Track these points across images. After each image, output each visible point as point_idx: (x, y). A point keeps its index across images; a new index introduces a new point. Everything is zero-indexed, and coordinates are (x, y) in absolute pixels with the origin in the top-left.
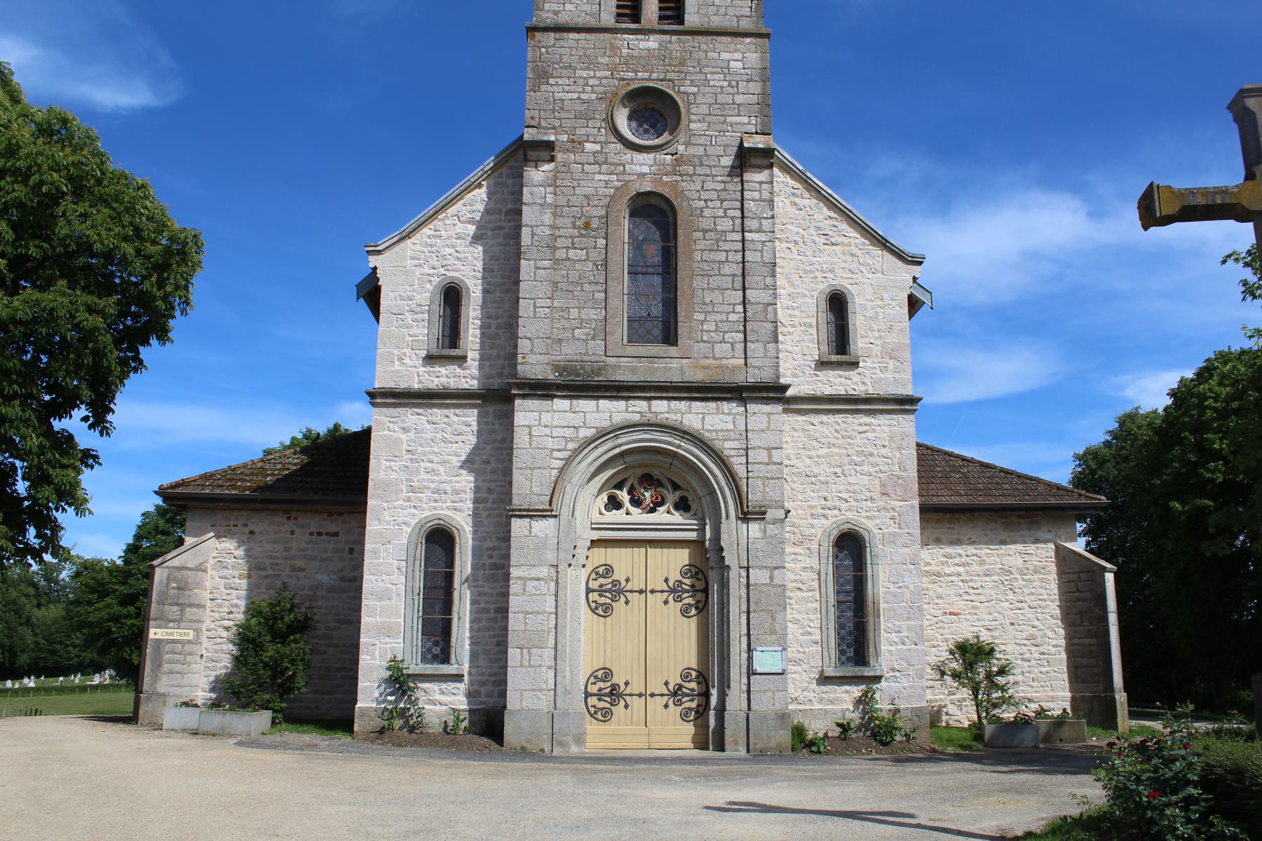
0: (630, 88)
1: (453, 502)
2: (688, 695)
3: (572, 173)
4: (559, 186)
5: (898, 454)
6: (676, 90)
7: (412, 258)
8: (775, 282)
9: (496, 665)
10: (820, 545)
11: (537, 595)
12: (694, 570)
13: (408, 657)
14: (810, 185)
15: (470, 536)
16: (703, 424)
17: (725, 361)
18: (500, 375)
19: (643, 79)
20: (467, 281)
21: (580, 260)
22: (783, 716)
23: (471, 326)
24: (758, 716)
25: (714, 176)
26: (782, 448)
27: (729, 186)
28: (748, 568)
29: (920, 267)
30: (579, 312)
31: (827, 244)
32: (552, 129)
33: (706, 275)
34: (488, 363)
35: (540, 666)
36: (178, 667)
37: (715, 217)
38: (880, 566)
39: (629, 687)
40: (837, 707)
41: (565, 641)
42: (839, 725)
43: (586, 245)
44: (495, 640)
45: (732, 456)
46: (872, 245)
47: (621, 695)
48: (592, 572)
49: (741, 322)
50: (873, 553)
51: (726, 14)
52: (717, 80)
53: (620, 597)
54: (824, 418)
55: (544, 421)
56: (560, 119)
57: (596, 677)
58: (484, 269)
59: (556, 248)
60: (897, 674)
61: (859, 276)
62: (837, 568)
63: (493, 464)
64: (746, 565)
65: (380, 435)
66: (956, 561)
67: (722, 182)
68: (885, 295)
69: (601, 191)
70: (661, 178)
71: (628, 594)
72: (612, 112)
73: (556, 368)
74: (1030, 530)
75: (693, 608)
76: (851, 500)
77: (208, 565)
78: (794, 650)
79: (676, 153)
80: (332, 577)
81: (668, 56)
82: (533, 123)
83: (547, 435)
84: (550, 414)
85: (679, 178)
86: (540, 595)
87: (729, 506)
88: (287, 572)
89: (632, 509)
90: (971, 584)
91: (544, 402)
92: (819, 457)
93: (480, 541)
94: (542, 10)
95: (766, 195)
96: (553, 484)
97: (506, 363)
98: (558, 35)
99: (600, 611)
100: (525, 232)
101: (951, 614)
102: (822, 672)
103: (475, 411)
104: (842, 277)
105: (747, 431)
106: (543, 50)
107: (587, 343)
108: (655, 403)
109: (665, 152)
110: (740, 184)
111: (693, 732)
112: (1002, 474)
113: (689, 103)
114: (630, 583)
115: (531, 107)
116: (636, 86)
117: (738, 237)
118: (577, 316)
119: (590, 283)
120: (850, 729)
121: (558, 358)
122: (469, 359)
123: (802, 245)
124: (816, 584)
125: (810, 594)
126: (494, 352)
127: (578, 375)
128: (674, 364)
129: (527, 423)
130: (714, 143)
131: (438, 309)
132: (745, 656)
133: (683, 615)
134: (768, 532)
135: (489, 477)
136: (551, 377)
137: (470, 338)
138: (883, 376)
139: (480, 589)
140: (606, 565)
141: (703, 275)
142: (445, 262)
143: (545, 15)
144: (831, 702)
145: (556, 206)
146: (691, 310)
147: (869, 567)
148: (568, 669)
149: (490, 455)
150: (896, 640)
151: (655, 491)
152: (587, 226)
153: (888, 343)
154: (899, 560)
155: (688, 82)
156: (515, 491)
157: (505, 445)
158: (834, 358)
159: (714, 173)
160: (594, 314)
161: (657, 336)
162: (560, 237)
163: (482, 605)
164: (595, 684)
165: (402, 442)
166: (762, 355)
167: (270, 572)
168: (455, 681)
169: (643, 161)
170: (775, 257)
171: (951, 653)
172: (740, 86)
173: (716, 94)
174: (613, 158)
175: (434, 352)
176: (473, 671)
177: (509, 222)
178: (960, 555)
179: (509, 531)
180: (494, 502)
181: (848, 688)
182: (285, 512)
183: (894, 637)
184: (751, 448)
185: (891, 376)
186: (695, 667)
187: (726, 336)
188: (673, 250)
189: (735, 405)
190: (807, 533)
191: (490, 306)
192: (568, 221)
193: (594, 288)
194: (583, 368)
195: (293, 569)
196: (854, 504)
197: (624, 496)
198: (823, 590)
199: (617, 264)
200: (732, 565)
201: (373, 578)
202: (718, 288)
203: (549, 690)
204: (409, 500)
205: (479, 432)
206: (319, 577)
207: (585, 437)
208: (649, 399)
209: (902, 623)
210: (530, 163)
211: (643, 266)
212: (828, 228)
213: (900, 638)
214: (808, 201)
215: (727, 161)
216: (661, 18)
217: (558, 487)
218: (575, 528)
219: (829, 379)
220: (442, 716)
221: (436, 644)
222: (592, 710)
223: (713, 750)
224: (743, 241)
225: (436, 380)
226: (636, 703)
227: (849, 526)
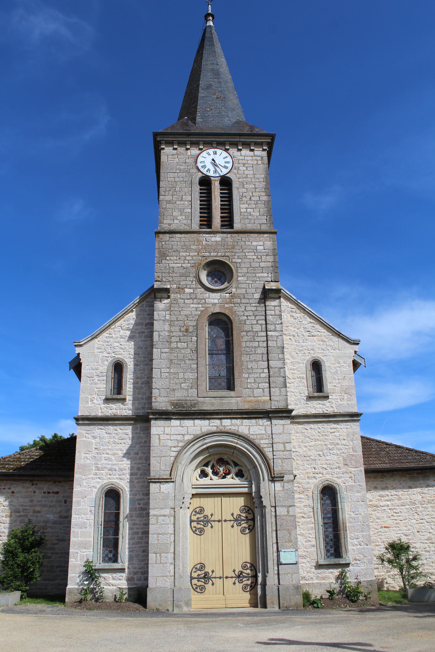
0: (207, 261)
1: (119, 475)
2: (246, 577)
3: (179, 304)
4: (173, 311)
5: (351, 443)
6: (231, 261)
7: (98, 348)
8: (284, 357)
9: (143, 563)
10: (313, 493)
11: (164, 524)
12: (247, 508)
13: (95, 560)
14: (300, 306)
15: (128, 493)
16: (249, 431)
17: (259, 398)
18: (144, 408)
19: (214, 256)
20: (126, 360)
21: (184, 348)
22: (298, 587)
23: (128, 383)
24: (284, 587)
25: (251, 304)
26: (291, 443)
28: (275, 507)
29: (358, 346)
30: (184, 375)
31: (310, 336)
32: (168, 282)
33: (248, 354)
34: (137, 402)
35: (166, 563)
38: (345, 503)
39: (214, 573)
40: (327, 581)
41: (179, 549)
42: (328, 591)
43: (187, 340)
44: (142, 549)
45: (265, 448)
46: (332, 335)
47: (209, 578)
48: (193, 511)
49: (267, 378)
50: (341, 497)
51: (254, 223)
52: (251, 256)
53: (208, 524)
54: (312, 426)
55: (166, 432)
56: (172, 277)
57: (196, 568)
58: (135, 354)
59: (172, 342)
60: (358, 562)
61: (327, 352)
62: (323, 505)
63: (140, 455)
64: (274, 505)
65: (81, 440)
66: (386, 498)
67: (255, 306)
68: (341, 361)
69: (194, 313)
70: (224, 305)
71: (212, 523)
72: (198, 273)
73: (172, 404)
74: (424, 480)
75: (247, 529)
76: (328, 468)
78: (302, 550)
79: (231, 293)
80: (55, 516)
81: (226, 244)
82: (159, 279)
83: (168, 439)
84: (170, 428)
85: (233, 305)
86: (166, 524)
87: (264, 474)
88: (31, 514)
89: (214, 477)
90: (394, 511)
91: (166, 422)
92: (310, 446)
93: (134, 495)
94: (162, 223)
95: (278, 312)
96: (172, 465)
97: (147, 402)
98: (171, 236)
99: (198, 532)
100: (155, 334)
101: (385, 527)
102: (318, 561)
103: (131, 427)
104: (318, 353)
105: (272, 434)
106: (163, 243)
107: (188, 391)
108: (224, 421)
109: (226, 292)
110: (264, 307)
111: (249, 597)
112: (407, 451)
114: (213, 516)
115: (157, 271)
116: (210, 260)
117: (264, 334)
118: (182, 377)
119: (189, 360)
120: (334, 594)
121: (173, 399)
122: (127, 400)
123: (297, 337)
124: (312, 514)
125: (309, 520)
126: (140, 396)
127: (184, 407)
128: (233, 400)
129: (158, 433)
130: (250, 287)
131: (111, 374)
132: (275, 554)
133: (242, 533)
134: (285, 487)
135: (138, 461)
136: (170, 409)
137: (128, 389)
138: (342, 403)
139: (134, 522)
140: (200, 507)
141: (247, 354)
142: (114, 350)
143: (164, 226)
144: (323, 579)
145: (171, 321)
146: (241, 373)
147: (339, 504)
148: (181, 564)
149: (139, 450)
150: (356, 543)
151: (225, 467)
152: (187, 330)
153: (344, 386)
154: (355, 499)
155: (236, 257)
156: (152, 469)
157: (146, 445)
158: (316, 394)
159: (251, 302)
160: (191, 376)
161: (224, 386)
163: (135, 530)
164: (196, 572)
165: (93, 444)
166: (278, 394)
167: (22, 514)
168: (120, 572)
169: (215, 297)
170: (283, 344)
171: (387, 549)
172: (263, 258)
173: (250, 262)
175: (109, 396)
176: (130, 566)
177: (147, 329)
178: (388, 495)
179: (149, 490)
180: (141, 475)
181: (332, 570)
182: (31, 481)
183: (355, 541)
184: (275, 443)
185: (346, 403)
186: (249, 561)
187: (260, 385)
188: (231, 342)
189: (265, 421)
190: (306, 487)
191: (138, 372)
192: (177, 328)
193: (191, 362)
194: (186, 404)
195: (35, 512)
196: (330, 470)
197: (209, 470)
198: (316, 517)
199: (203, 350)
201: (77, 516)
202: (255, 360)
203: (171, 576)
204: (96, 474)
205: (133, 438)
206: (48, 516)
207: (188, 440)
208: (221, 419)
209: (359, 533)
210: (157, 299)
211: (216, 350)
212: (310, 328)
213: (358, 542)
214: (299, 315)
215: (257, 296)
216: (222, 226)
217: (174, 466)
218: (184, 488)
219: (314, 405)
220: (114, 592)
221: (110, 552)
223: (260, 608)
224: (267, 336)
225: (110, 411)
226: (218, 582)
227: (328, 482)
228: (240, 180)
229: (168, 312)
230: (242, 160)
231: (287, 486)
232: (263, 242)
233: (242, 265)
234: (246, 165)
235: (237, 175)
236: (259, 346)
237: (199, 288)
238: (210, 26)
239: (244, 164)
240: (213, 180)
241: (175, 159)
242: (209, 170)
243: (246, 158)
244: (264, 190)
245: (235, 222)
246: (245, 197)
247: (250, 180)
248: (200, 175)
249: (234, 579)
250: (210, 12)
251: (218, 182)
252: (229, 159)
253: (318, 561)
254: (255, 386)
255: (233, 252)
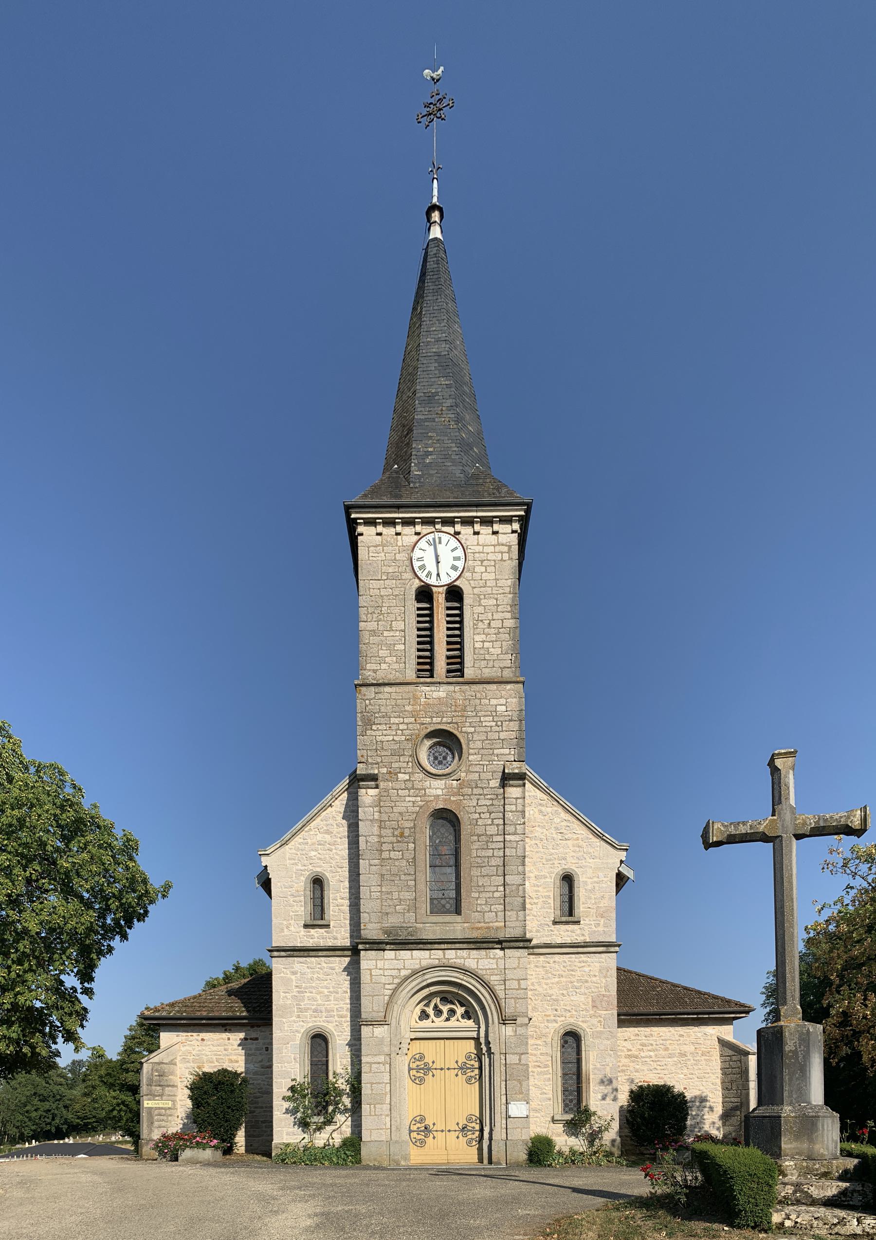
0: (428, 730)
2: (471, 1131)
3: (390, 797)
17: (491, 924)
19: (437, 723)
27: (495, 802)
35: (381, 1115)
36: (163, 1124)
37: (485, 825)
47: (430, 1131)
51: (494, 667)
52: (488, 721)
55: (379, 966)
56: (381, 756)
59: (381, 851)
71: (434, 1071)
77: (177, 1061)
85: (462, 798)
87: (493, 1016)
100: (361, 839)
108: (447, 952)
113: (469, 741)
116: (432, 729)
121: (386, 925)
128: (459, 927)
132: (504, 1107)
136: (383, 938)
152: (402, 835)
155: (468, 724)
158: (564, 919)
159: (485, 793)
160: (407, 895)
162: (384, 843)
170: (525, 852)
172: (504, 725)
173: (486, 732)
174: (418, 785)
187: (492, 907)
192: (389, 832)
197: (430, 1011)
200: (495, 1052)
201: (279, 1065)
215: (495, 783)
222: (414, 1140)
228: (476, 591)
229: (376, 809)
230: (479, 553)
231: (520, 1031)
232: (506, 699)
233: (475, 736)
234: (485, 563)
235: (471, 582)
236: (493, 856)
237: (418, 773)
238: (436, 239)
239: (482, 561)
240: (436, 592)
241: (380, 555)
242: (429, 574)
243: (486, 549)
244: (509, 609)
245: (465, 666)
246: (482, 621)
247: (489, 590)
248: (417, 583)
249: (458, 1132)
250: (435, 200)
251: (444, 595)
252: (460, 553)
253: (553, 1117)
254: (486, 909)
255: (463, 716)
